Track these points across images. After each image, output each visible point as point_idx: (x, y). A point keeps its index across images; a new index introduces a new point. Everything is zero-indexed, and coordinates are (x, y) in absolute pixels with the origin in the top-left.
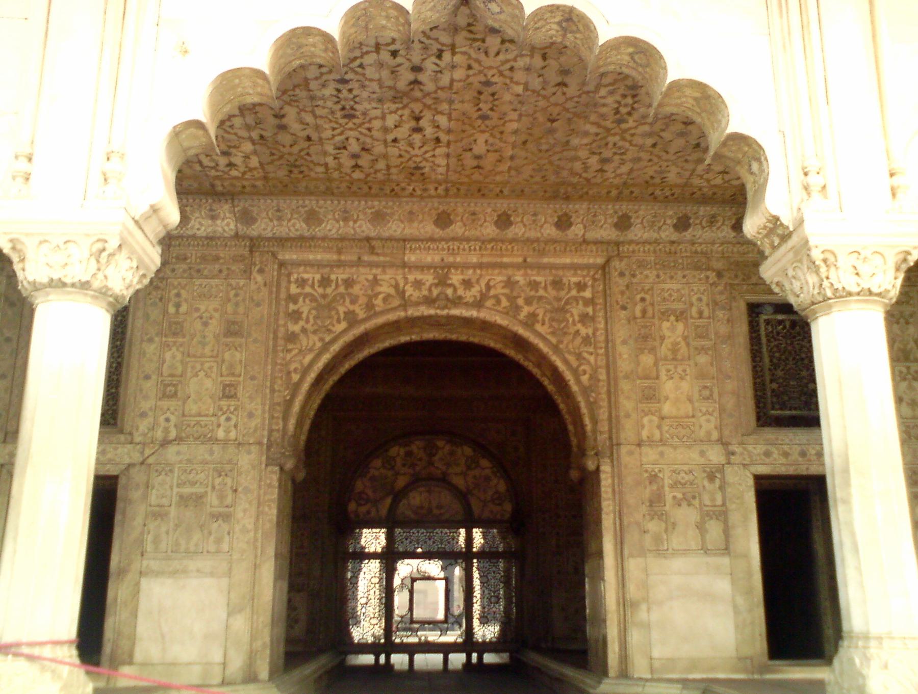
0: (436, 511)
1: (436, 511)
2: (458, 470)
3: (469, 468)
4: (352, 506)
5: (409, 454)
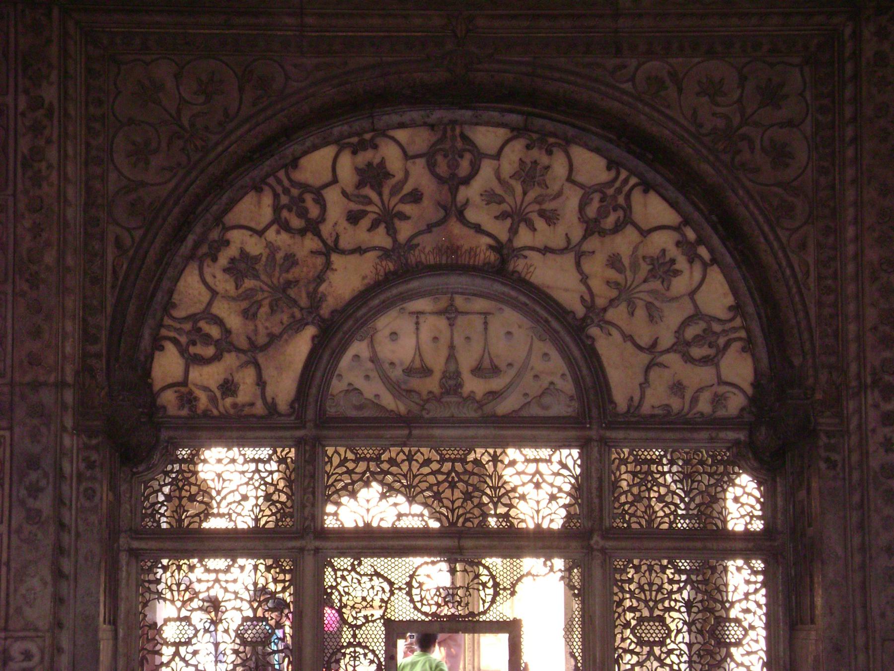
0: (473, 386)
1: (473, 386)
2: (553, 236)
3: (592, 228)
4: (168, 365)
5: (373, 176)
